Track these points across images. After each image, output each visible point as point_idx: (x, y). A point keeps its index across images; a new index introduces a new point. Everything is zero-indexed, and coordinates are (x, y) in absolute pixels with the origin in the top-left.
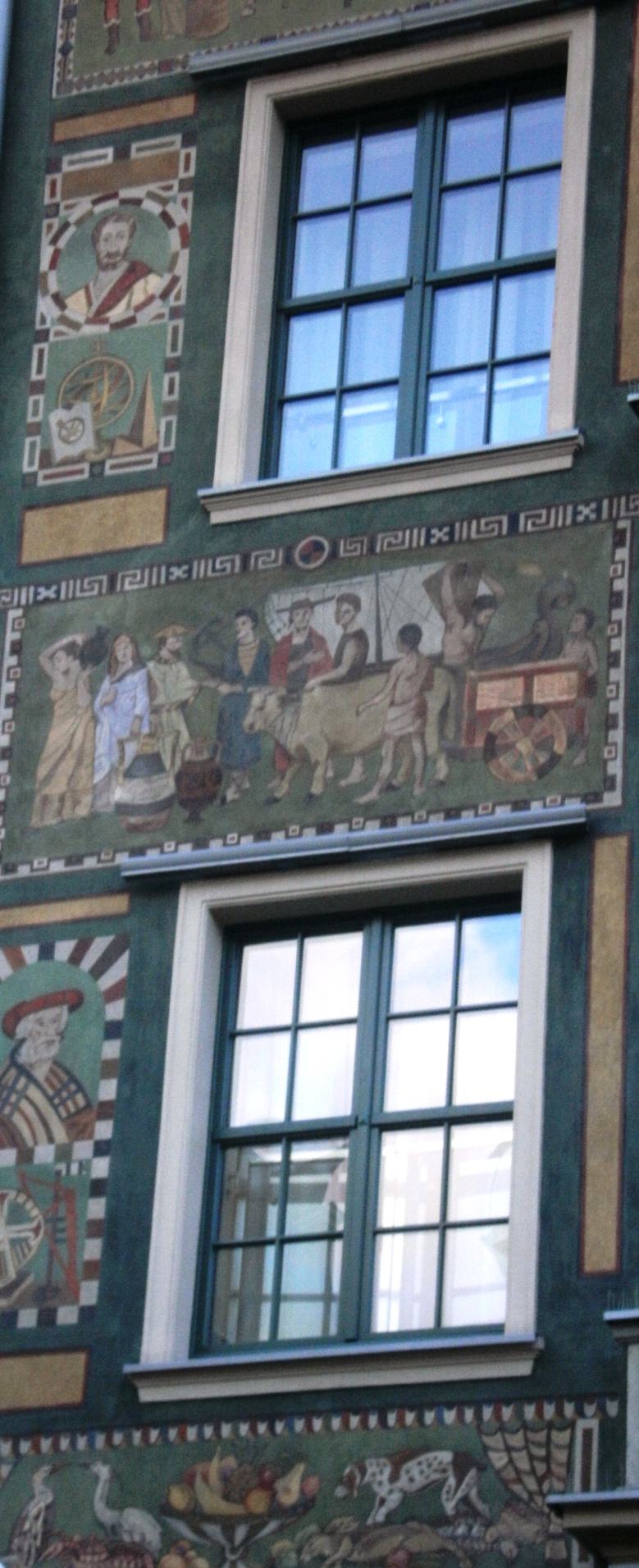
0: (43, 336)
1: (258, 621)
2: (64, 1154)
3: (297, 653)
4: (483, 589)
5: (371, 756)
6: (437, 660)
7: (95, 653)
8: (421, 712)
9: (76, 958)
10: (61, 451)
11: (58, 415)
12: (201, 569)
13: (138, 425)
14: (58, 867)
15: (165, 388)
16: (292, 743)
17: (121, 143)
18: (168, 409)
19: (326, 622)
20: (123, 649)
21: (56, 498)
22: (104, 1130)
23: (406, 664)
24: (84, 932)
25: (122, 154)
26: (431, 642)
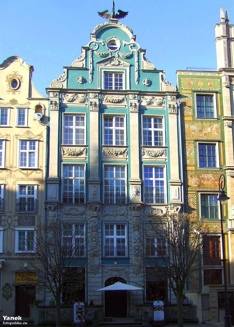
1: (201, 176)
2: (194, 207)
3: (204, 178)
4: (215, 176)
5: (209, 185)
6: (213, 180)
7: (191, 176)
8: (212, 183)
9: (193, 195)
13: (192, 162)
14: (191, 190)
15: (194, 160)
18: (194, 161)
19: (206, 176)
20: (193, 176)
22: (196, 206)
23: (211, 180)
24: (193, 194)
25: (189, 144)
26: (212, 179)
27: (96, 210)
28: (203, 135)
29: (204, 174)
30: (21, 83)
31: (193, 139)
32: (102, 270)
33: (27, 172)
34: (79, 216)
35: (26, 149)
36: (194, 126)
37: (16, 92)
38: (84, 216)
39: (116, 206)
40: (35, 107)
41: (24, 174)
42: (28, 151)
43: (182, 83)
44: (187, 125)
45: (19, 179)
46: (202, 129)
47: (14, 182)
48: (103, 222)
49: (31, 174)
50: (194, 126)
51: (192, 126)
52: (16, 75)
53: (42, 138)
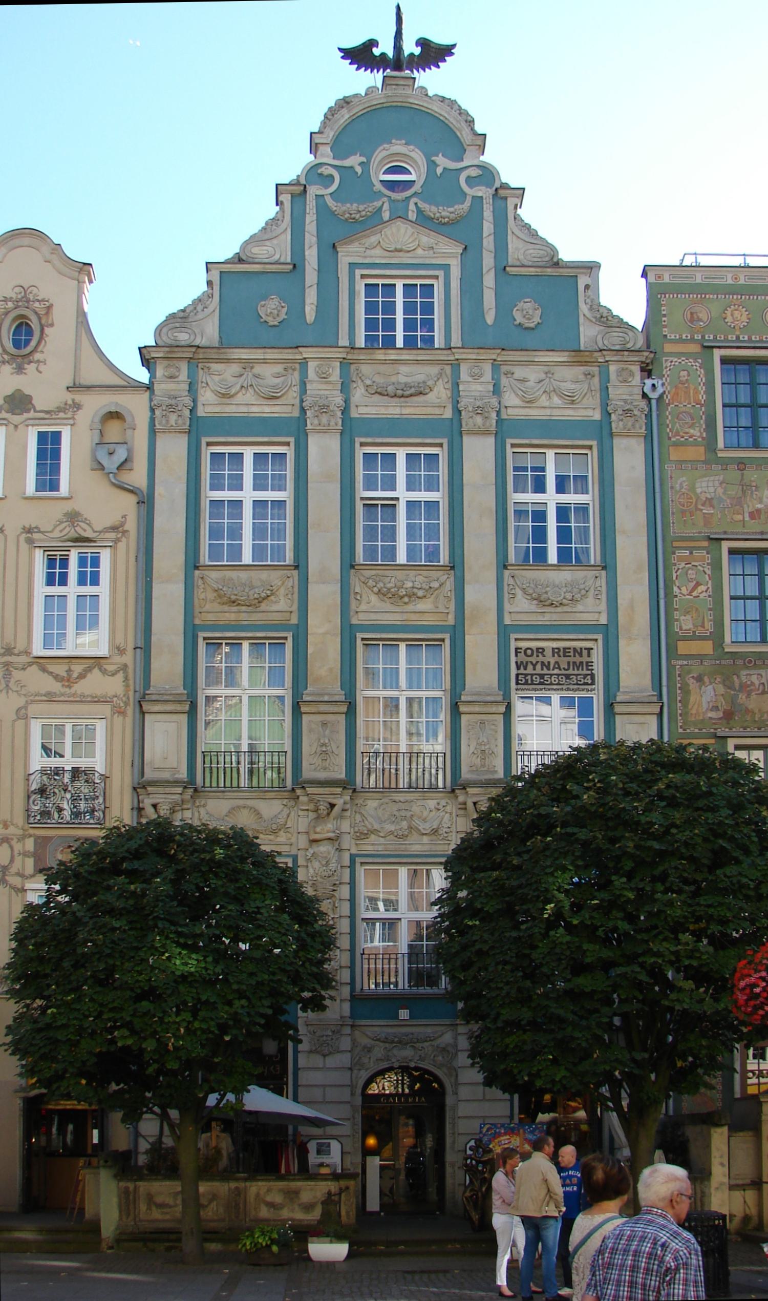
1: (738, 677)
7: (699, 679)
10: (684, 627)
11: (682, 618)
12: (723, 662)
13: (703, 623)
14: (697, 731)
15: (709, 616)
16: (750, 707)
17: (691, 550)
19: (754, 679)
20: (706, 679)
21: (684, 639)
25: (691, 553)
27: (328, 814)
28: (747, 518)
29: (748, 668)
30: (47, 330)
31: (706, 531)
32: (354, 1041)
40: (97, 419)
41: (57, 677)
42: (72, 589)
43: (665, 316)
44: (684, 479)
45: (37, 698)
46: (744, 492)
47: (18, 710)
48: (358, 860)
49: (82, 676)
50: (711, 484)
52: (28, 301)
53: (124, 539)
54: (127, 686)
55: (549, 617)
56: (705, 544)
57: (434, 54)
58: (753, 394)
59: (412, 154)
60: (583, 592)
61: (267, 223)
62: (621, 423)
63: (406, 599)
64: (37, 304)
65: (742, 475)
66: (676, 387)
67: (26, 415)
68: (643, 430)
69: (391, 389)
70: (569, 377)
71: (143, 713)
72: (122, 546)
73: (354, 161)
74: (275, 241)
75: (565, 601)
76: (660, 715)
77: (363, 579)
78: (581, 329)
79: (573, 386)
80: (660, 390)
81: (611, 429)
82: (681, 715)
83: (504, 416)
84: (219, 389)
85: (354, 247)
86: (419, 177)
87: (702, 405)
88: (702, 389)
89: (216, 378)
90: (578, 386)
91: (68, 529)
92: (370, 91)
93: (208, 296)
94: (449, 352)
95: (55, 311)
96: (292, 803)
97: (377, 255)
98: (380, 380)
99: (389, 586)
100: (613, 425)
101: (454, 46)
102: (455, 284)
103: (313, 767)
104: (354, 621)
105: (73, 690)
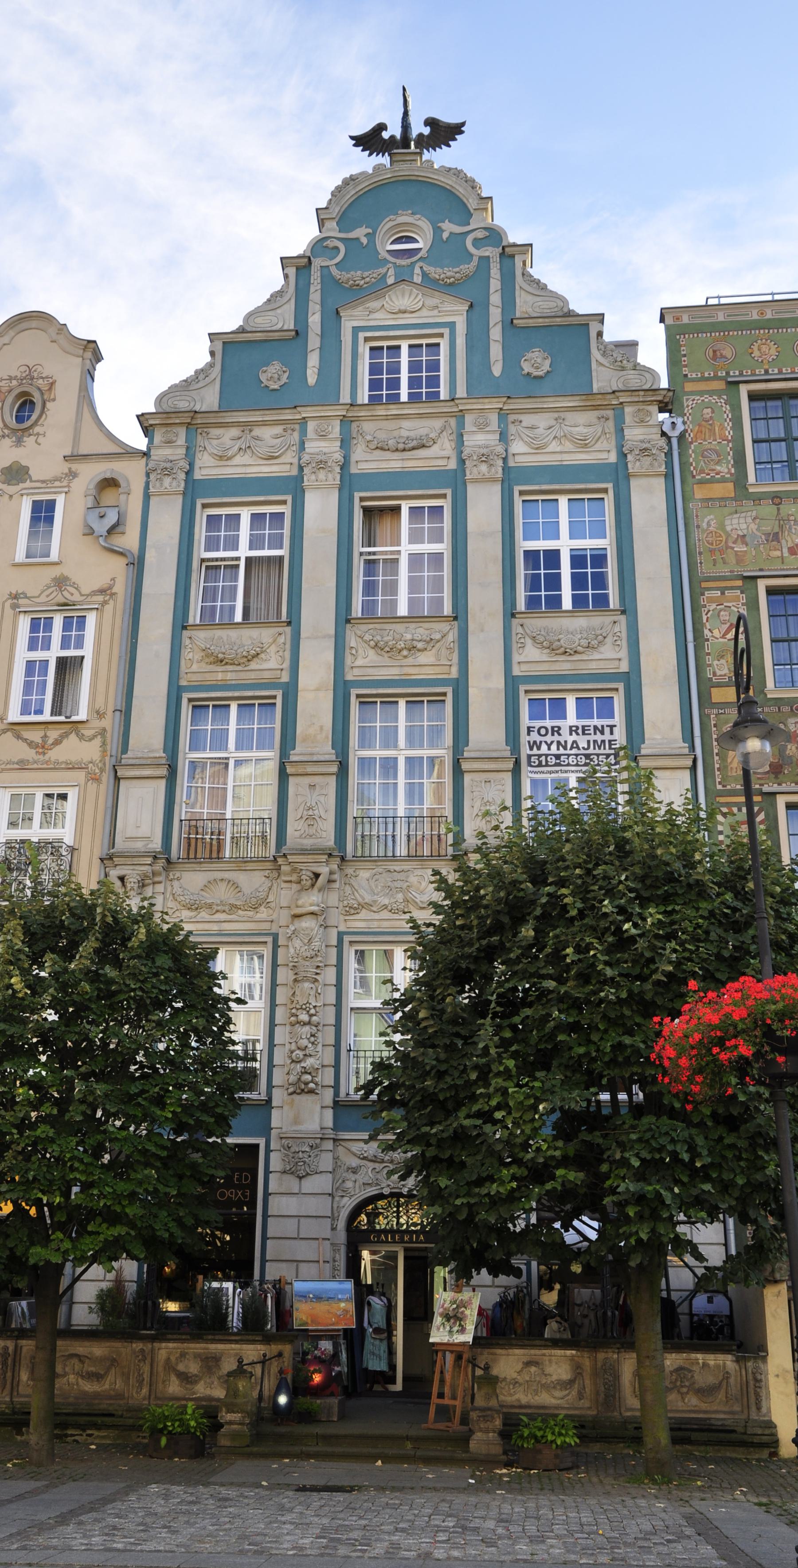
0: (708, 640)
10: (719, 673)
11: (716, 662)
17: (723, 590)
25: (723, 593)
27: (313, 885)
28: (786, 554)
31: (739, 570)
32: (336, 1159)
33: (46, 736)
34: (240, 912)
35: (47, 646)
36: (742, 521)
37: (25, 439)
38: (263, 913)
39: (406, 867)
40: (92, 486)
41: (31, 744)
42: (55, 652)
43: (685, 356)
45: (8, 766)
46: (781, 527)
48: (347, 939)
49: (57, 742)
50: (742, 521)
51: (735, 521)
52: (32, 379)
53: (111, 602)
54: (104, 751)
55: (564, 666)
56: (739, 583)
57: (443, 133)
58: (788, 428)
59: (419, 223)
60: (600, 638)
61: (272, 296)
62: (638, 463)
63: (405, 653)
64: (41, 381)
65: (778, 509)
66: (700, 425)
67: (22, 485)
68: (663, 468)
69: (391, 443)
70: (582, 423)
71: (117, 779)
72: (109, 608)
73: (361, 233)
74: (279, 311)
75: (580, 649)
76: (694, 768)
77: (359, 633)
78: (594, 374)
79: (585, 430)
80: (680, 428)
81: (627, 469)
82: (719, 769)
83: (511, 464)
84: (215, 452)
85: (359, 311)
86: (425, 244)
87: (729, 441)
88: (728, 425)
89: (215, 442)
90: (591, 429)
91: (55, 594)
92: (378, 168)
93: (211, 365)
94: (452, 403)
95: (58, 387)
96: (275, 874)
97: (381, 318)
98: (381, 436)
99: (386, 639)
100: (630, 465)
101: (463, 124)
102: (461, 341)
103: (297, 834)
104: (349, 677)
105: (47, 757)
